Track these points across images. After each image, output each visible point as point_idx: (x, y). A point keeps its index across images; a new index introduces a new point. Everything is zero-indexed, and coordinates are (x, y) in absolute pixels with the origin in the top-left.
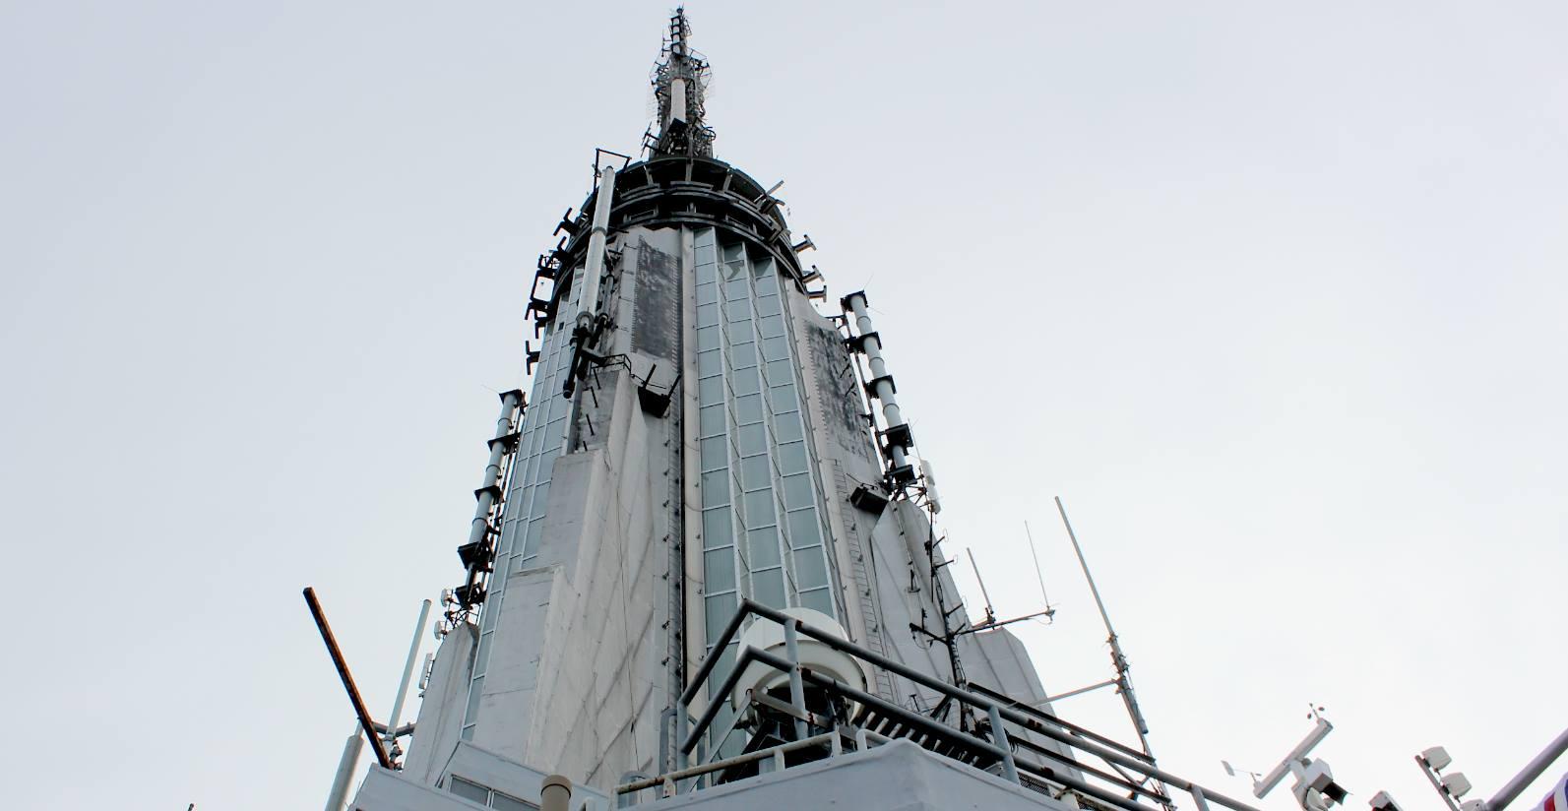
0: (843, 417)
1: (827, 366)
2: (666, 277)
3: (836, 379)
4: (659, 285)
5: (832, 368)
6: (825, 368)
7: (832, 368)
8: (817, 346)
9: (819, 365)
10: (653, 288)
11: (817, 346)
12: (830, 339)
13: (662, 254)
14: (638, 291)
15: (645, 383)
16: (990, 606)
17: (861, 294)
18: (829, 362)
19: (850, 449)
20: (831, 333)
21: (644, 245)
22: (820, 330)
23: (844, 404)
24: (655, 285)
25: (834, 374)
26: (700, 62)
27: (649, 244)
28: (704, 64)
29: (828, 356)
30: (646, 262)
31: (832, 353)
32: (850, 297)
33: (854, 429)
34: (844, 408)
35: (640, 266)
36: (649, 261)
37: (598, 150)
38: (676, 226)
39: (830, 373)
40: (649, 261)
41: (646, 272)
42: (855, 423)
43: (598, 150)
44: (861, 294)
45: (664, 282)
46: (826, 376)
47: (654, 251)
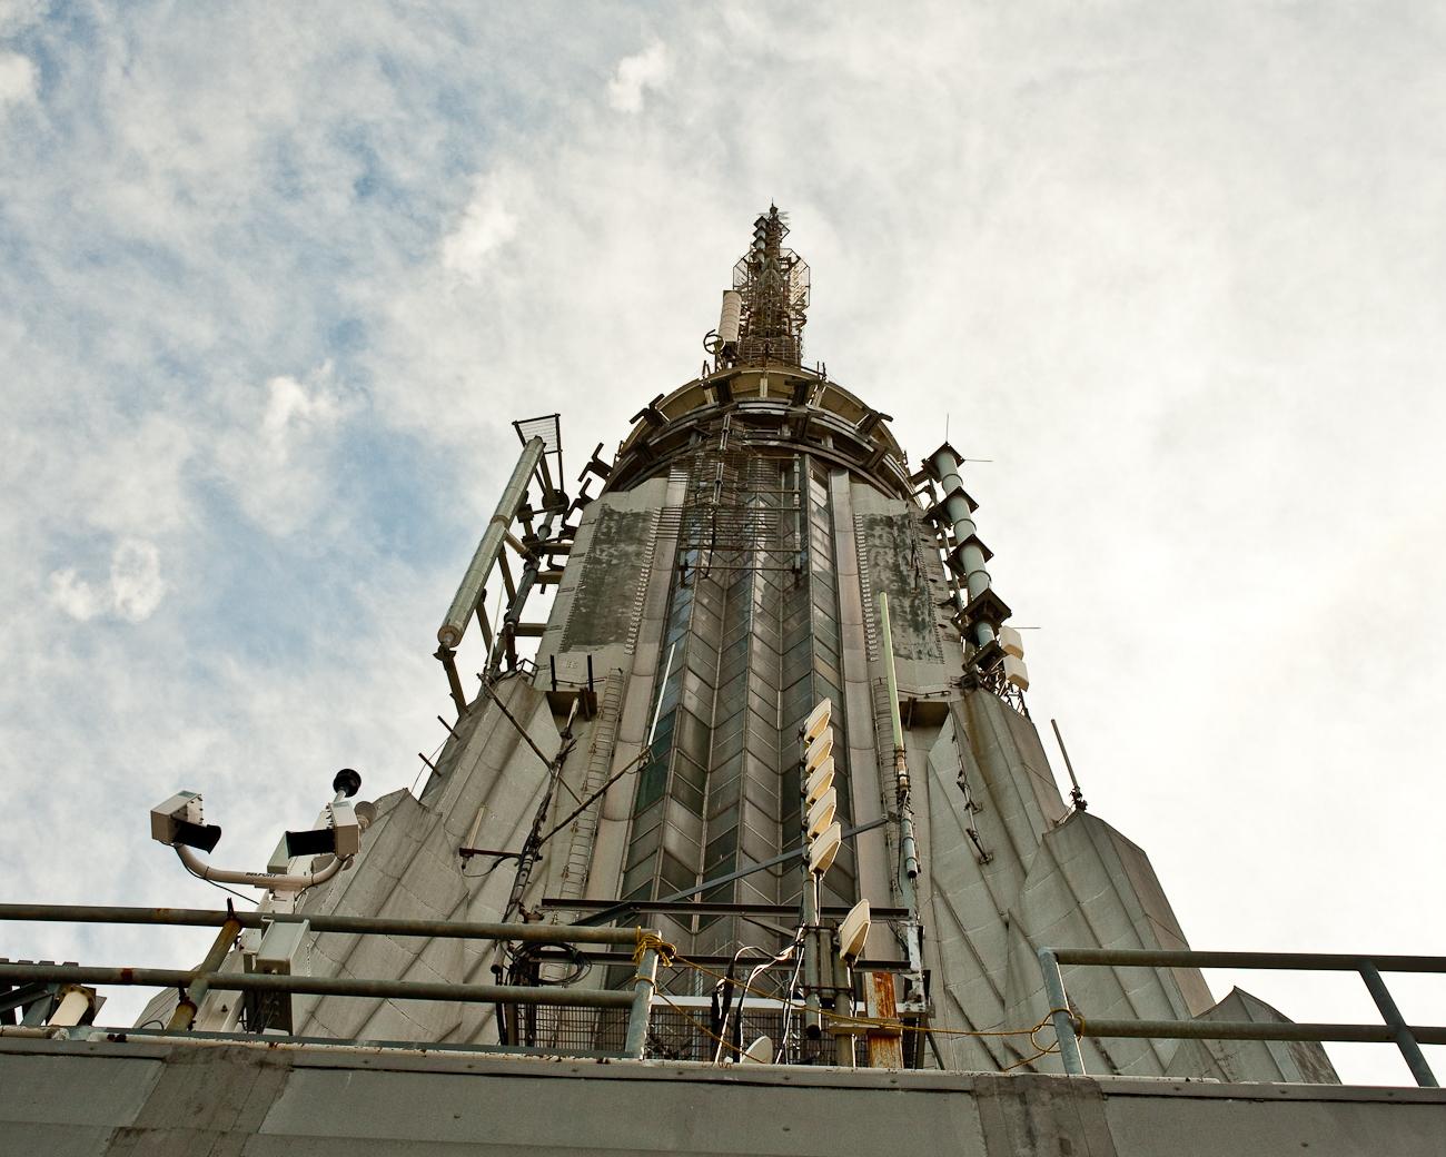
0: (909, 617)
1: (891, 561)
2: (631, 540)
3: (905, 573)
4: (626, 555)
5: (900, 560)
6: (886, 567)
7: (900, 560)
8: (877, 542)
9: (876, 564)
10: (614, 562)
11: (877, 542)
12: (903, 525)
13: (637, 515)
14: (585, 575)
15: (554, 682)
16: (1076, 787)
17: (946, 448)
18: (896, 555)
19: (915, 655)
20: (905, 517)
21: (608, 513)
22: (890, 518)
23: (913, 601)
24: (616, 557)
25: (903, 568)
26: (789, 259)
27: (617, 510)
28: (794, 260)
29: (896, 547)
30: (607, 534)
31: (903, 541)
32: (934, 458)
33: (924, 628)
34: (912, 606)
35: (596, 541)
36: (613, 530)
37: (516, 424)
38: (664, 473)
39: (896, 568)
40: (613, 530)
41: (605, 546)
42: (927, 619)
43: (516, 424)
44: (946, 448)
45: (631, 549)
46: (886, 575)
47: (623, 516)
